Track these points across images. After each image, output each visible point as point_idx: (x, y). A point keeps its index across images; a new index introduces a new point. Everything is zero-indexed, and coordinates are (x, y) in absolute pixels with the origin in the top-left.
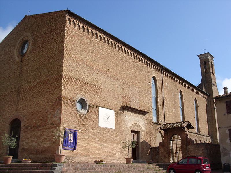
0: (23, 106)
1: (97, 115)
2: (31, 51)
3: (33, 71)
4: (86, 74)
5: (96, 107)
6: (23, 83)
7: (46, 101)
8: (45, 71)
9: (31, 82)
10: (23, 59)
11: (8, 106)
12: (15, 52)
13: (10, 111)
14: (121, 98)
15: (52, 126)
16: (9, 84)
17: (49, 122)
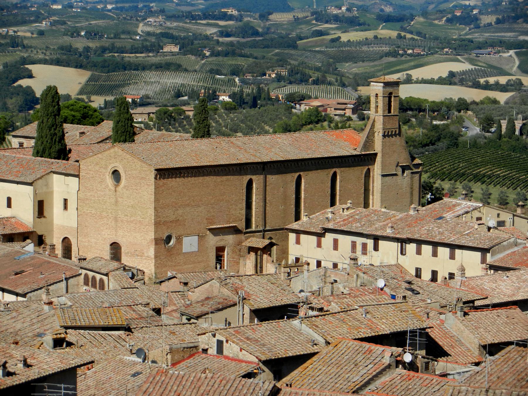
0: (122, 234)
1: (182, 245)
2: (125, 187)
3: (129, 207)
4: (172, 213)
5: (179, 240)
6: (120, 214)
7: (142, 238)
8: (139, 213)
9: (127, 216)
10: (117, 189)
11: (107, 229)
12: (108, 177)
13: (109, 233)
14: (205, 221)
15: (148, 258)
16: (104, 207)
17: (145, 254)
